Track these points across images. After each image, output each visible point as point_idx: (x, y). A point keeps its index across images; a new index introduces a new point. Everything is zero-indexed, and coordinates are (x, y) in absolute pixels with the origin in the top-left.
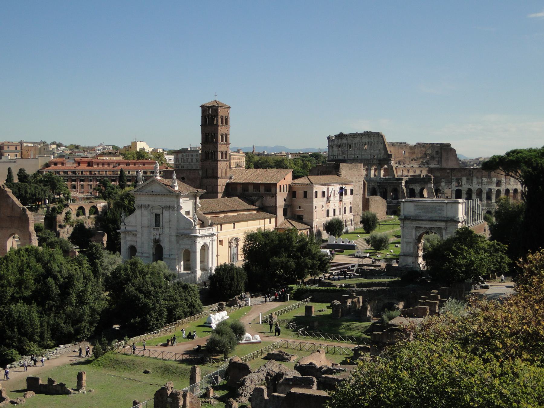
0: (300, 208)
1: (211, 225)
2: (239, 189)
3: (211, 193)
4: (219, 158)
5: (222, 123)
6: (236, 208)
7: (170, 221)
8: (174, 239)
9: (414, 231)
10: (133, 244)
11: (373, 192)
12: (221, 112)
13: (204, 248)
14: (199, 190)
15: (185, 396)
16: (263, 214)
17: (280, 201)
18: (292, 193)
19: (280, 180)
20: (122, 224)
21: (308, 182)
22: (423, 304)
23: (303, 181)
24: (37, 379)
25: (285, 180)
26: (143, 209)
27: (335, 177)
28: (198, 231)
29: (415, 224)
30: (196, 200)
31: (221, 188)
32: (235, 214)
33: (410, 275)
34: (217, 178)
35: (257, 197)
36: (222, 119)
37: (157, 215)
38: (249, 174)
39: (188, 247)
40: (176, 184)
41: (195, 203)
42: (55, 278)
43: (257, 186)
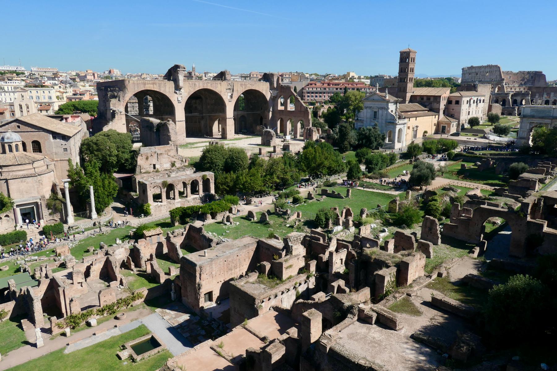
1: (405, 118)
2: (418, 99)
3: (404, 101)
6: (417, 109)
7: (382, 115)
8: (384, 125)
9: (528, 125)
11: (497, 102)
12: (412, 55)
13: (400, 130)
17: (442, 106)
18: (449, 102)
22: (541, 167)
23: (457, 94)
27: (474, 92)
29: (531, 120)
33: (525, 150)
35: (429, 104)
37: (375, 112)
39: (391, 129)
43: (429, 97)
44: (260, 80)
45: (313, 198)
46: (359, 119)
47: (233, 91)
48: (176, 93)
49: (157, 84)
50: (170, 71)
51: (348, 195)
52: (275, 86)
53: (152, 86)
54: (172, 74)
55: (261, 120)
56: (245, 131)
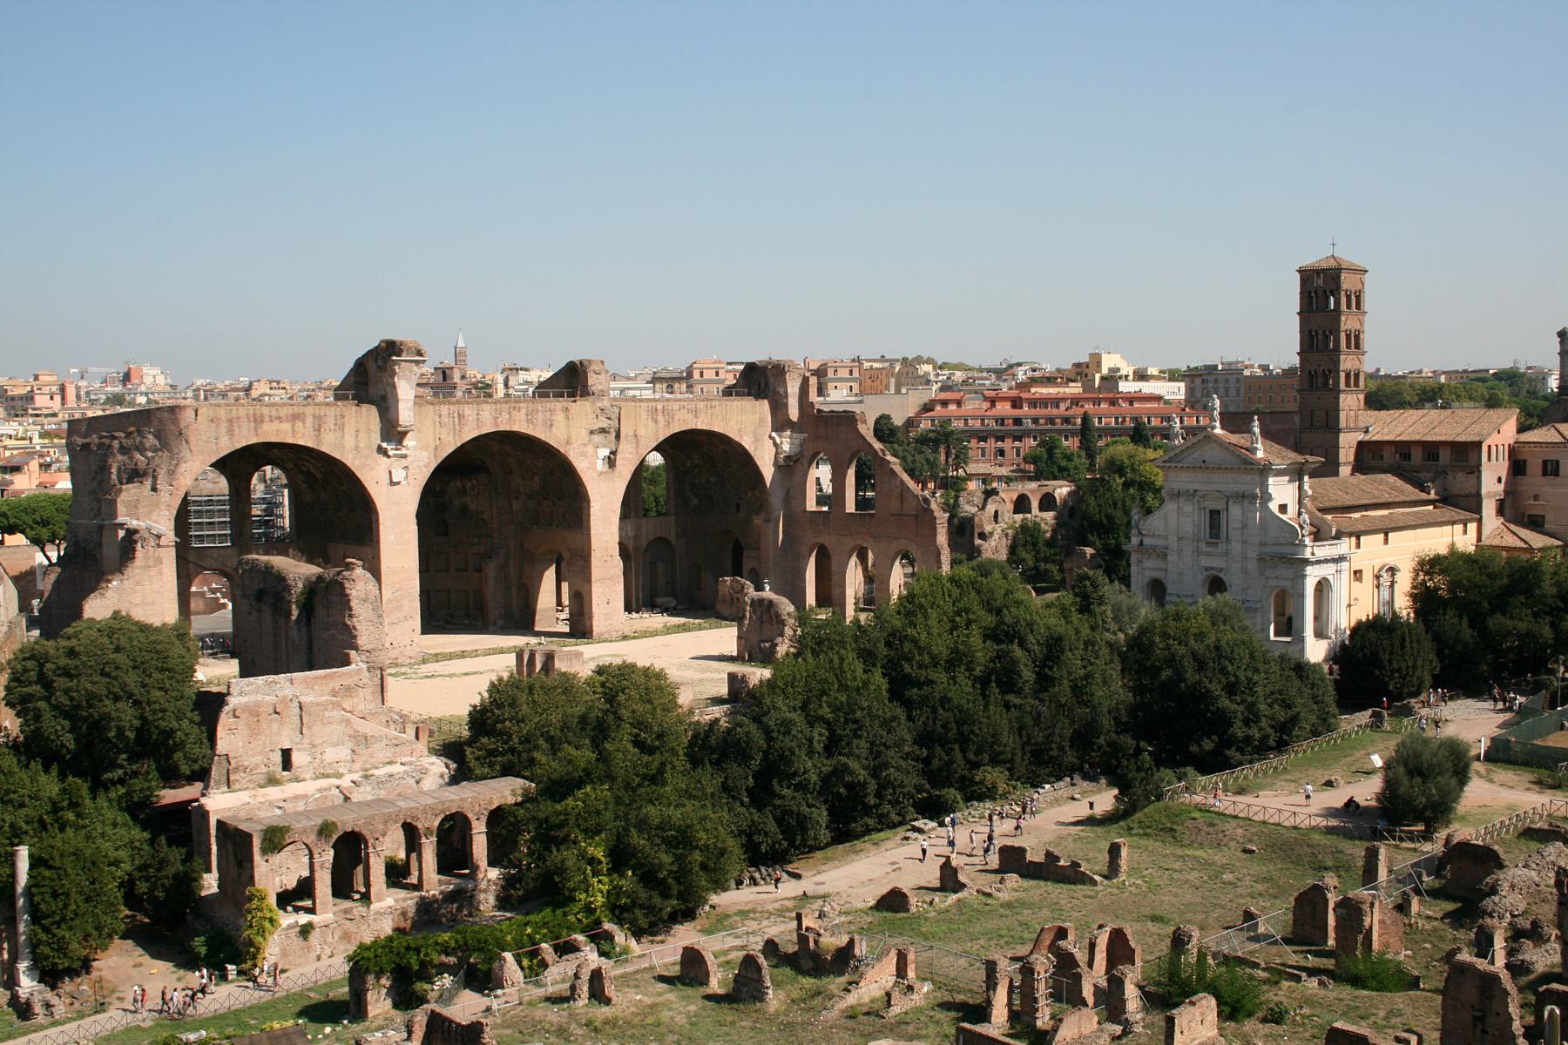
0: (1536, 498)
1: (1338, 536)
2: (1389, 456)
3: (1329, 468)
4: (1342, 386)
5: (1349, 306)
6: (1386, 497)
7: (1244, 526)
8: (1253, 566)
10: (1157, 575)
12: (1347, 281)
14: (1311, 459)
15: (1372, 905)
16: (1449, 512)
18: (1517, 466)
19: (1489, 434)
20: (1134, 531)
21: (1559, 439)
24: (1022, 851)
25: (1500, 432)
26: (1182, 499)
28: (1309, 550)
30: (1300, 480)
31: (1346, 453)
32: (1385, 512)
34: (1337, 431)
35: (1440, 473)
36: (1349, 297)
37: (1214, 514)
38: (1411, 421)
39: (1286, 584)
40: (1259, 446)
41: (1300, 488)
42: (1022, 644)
43: (1431, 450)
44: (728, 392)
45: (963, 886)
46: (1147, 541)
47: (618, 437)
48: (384, 452)
49: (309, 420)
50: (361, 366)
51: (1113, 870)
52: (794, 413)
53: (286, 426)
54: (369, 380)
55: (738, 556)
56: (671, 602)
